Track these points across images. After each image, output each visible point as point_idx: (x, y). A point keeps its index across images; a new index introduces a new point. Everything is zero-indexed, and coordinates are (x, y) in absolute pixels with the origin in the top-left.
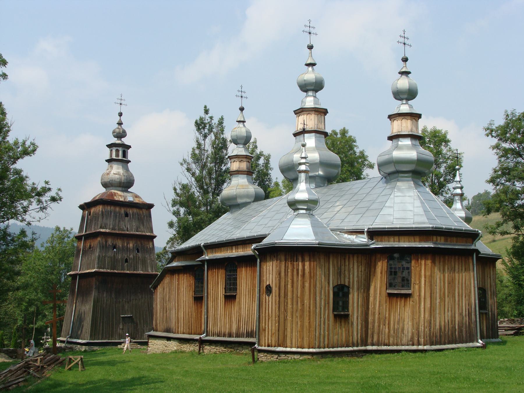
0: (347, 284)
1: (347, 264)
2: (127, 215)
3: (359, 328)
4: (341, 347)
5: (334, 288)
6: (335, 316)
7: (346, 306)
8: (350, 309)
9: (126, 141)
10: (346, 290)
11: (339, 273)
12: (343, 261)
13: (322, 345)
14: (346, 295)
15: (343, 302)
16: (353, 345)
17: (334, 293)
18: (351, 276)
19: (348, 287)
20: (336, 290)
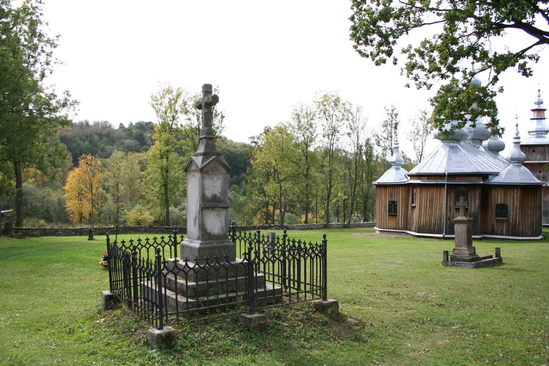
0: (396, 200)
1: (396, 191)
2: (534, 151)
3: (403, 221)
4: (393, 229)
5: (389, 202)
6: (389, 215)
7: (395, 211)
8: (398, 212)
9: (542, 107)
10: (396, 203)
11: (391, 195)
12: (394, 190)
13: (383, 227)
14: (396, 205)
15: (394, 209)
16: (399, 229)
17: (389, 205)
18: (398, 197)
19: (397, 202)
20: (390, 203)
